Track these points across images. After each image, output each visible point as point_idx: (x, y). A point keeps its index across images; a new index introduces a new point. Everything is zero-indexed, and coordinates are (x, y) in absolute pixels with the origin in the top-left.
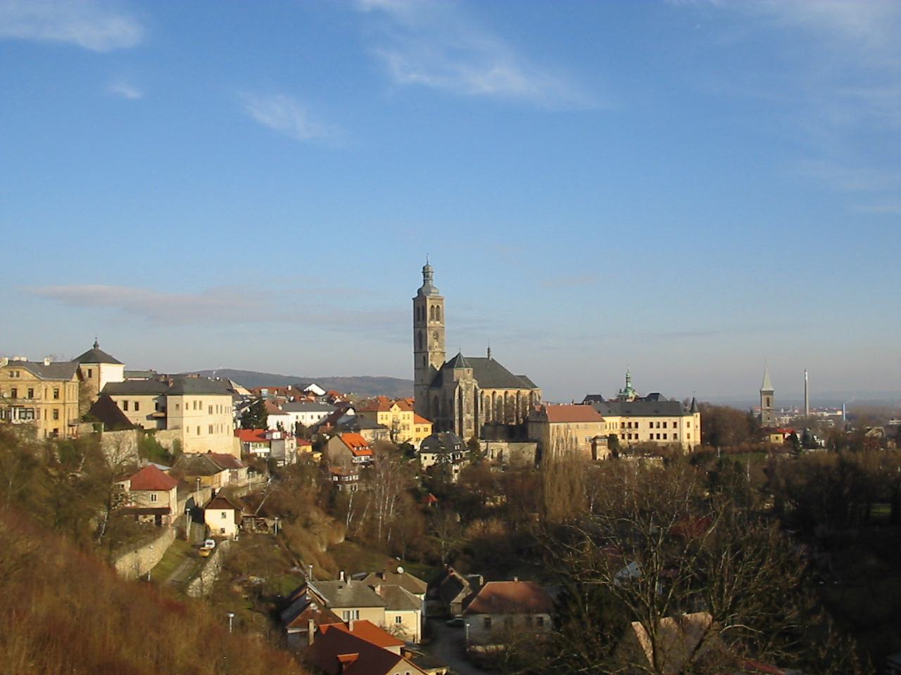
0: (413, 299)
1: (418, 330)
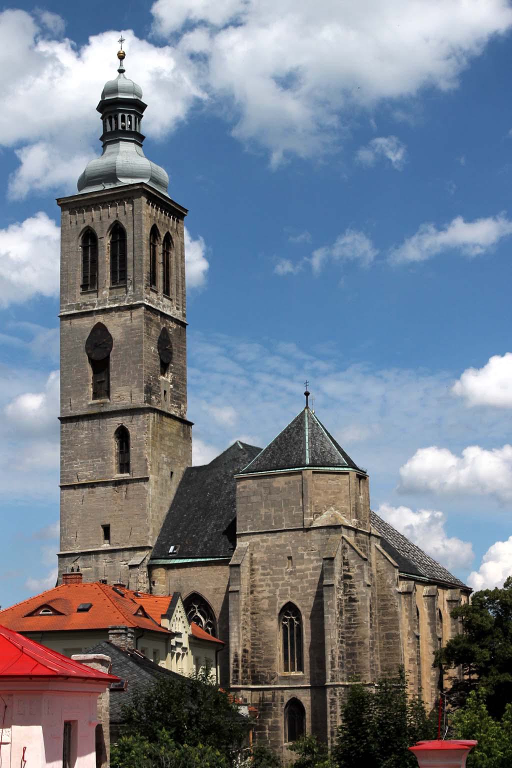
1: (88, 323)
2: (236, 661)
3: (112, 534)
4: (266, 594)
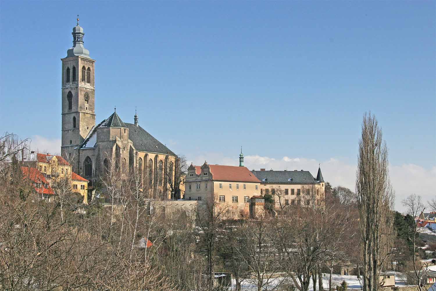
0: (62, 60)
1: (67, 91)
2: (93, 171)
3: (72, 142)
4: (101, 156)
